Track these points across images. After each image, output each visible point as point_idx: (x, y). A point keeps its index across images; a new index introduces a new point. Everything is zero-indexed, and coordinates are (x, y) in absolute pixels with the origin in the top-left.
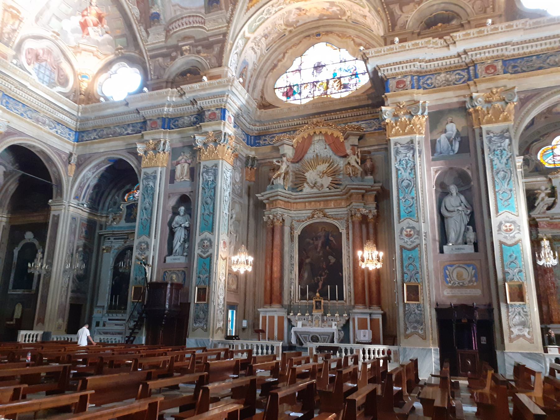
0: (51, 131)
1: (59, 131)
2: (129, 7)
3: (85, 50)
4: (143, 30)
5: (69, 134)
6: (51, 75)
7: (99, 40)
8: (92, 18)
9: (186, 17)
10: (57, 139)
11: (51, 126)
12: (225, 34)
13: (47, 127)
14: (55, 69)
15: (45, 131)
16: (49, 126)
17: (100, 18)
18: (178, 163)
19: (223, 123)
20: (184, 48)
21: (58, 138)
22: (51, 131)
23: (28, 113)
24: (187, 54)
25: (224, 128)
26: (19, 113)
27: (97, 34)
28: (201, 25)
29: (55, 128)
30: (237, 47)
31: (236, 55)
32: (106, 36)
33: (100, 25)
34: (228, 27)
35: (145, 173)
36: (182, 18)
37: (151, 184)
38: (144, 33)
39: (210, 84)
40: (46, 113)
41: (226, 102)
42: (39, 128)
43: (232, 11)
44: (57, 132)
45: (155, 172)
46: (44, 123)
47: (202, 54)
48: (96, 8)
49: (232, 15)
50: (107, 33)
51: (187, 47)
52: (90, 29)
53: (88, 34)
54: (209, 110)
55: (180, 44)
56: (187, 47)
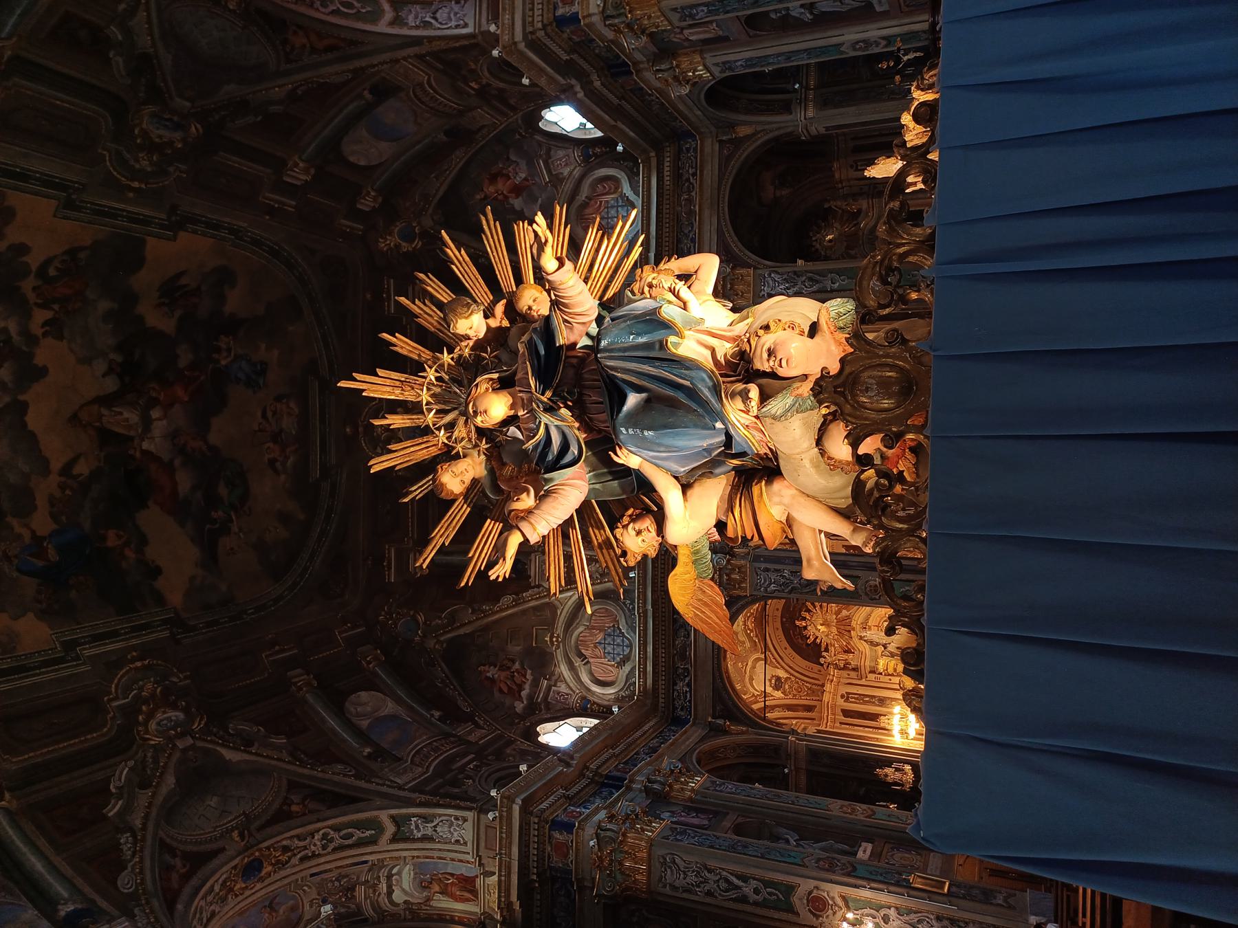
0: (697, 186)
1: (691, 171)
2: (459, 163)
3: (549, 172)
4: (480, 134)
5: (688, 150)
6: (613, 207)
7: (524, 162)
8: (502, 186)
9: (426, 106)
10: (705, 172)
11: (688, 187)
12: (420, 57)
13: (693, 194)
14: (601, 202)
15: (701, 196)
16: (689, 192)
17: (493, 179)
18: (687, 39)
19: (587, 21)
20: (476, 87)
21: (701, 171)
22: (697, 186)
23: (686, 231)
24: (484, 81)
25: (594, 14)
26: (692, 245)
27: (517, 170)
28: (426, 86)
29: (688, 180)
30: (427, 25)
31: (438, 15)
32: (513, 158)
33: (504, 172)
34: (405, 59)
35: (722, 71)
36: (431, 108)
37: (740, 63)
38: (485, 131)
39: (521, 53)
40: (674, 203)
41: (544, 27)
42: (700, 210)
43: (374, 66)
44: (694, 174)
45: (717, 65)
46: (690, 201)
47: (473, 66)
48: (485, 190)
49: (382, 64)
50: (508, 159)
51: (473, 85)
52: (518, 180)
53: (526, 179)
54: (570, 39)
55: (473, 92)
56: (473, 85)
